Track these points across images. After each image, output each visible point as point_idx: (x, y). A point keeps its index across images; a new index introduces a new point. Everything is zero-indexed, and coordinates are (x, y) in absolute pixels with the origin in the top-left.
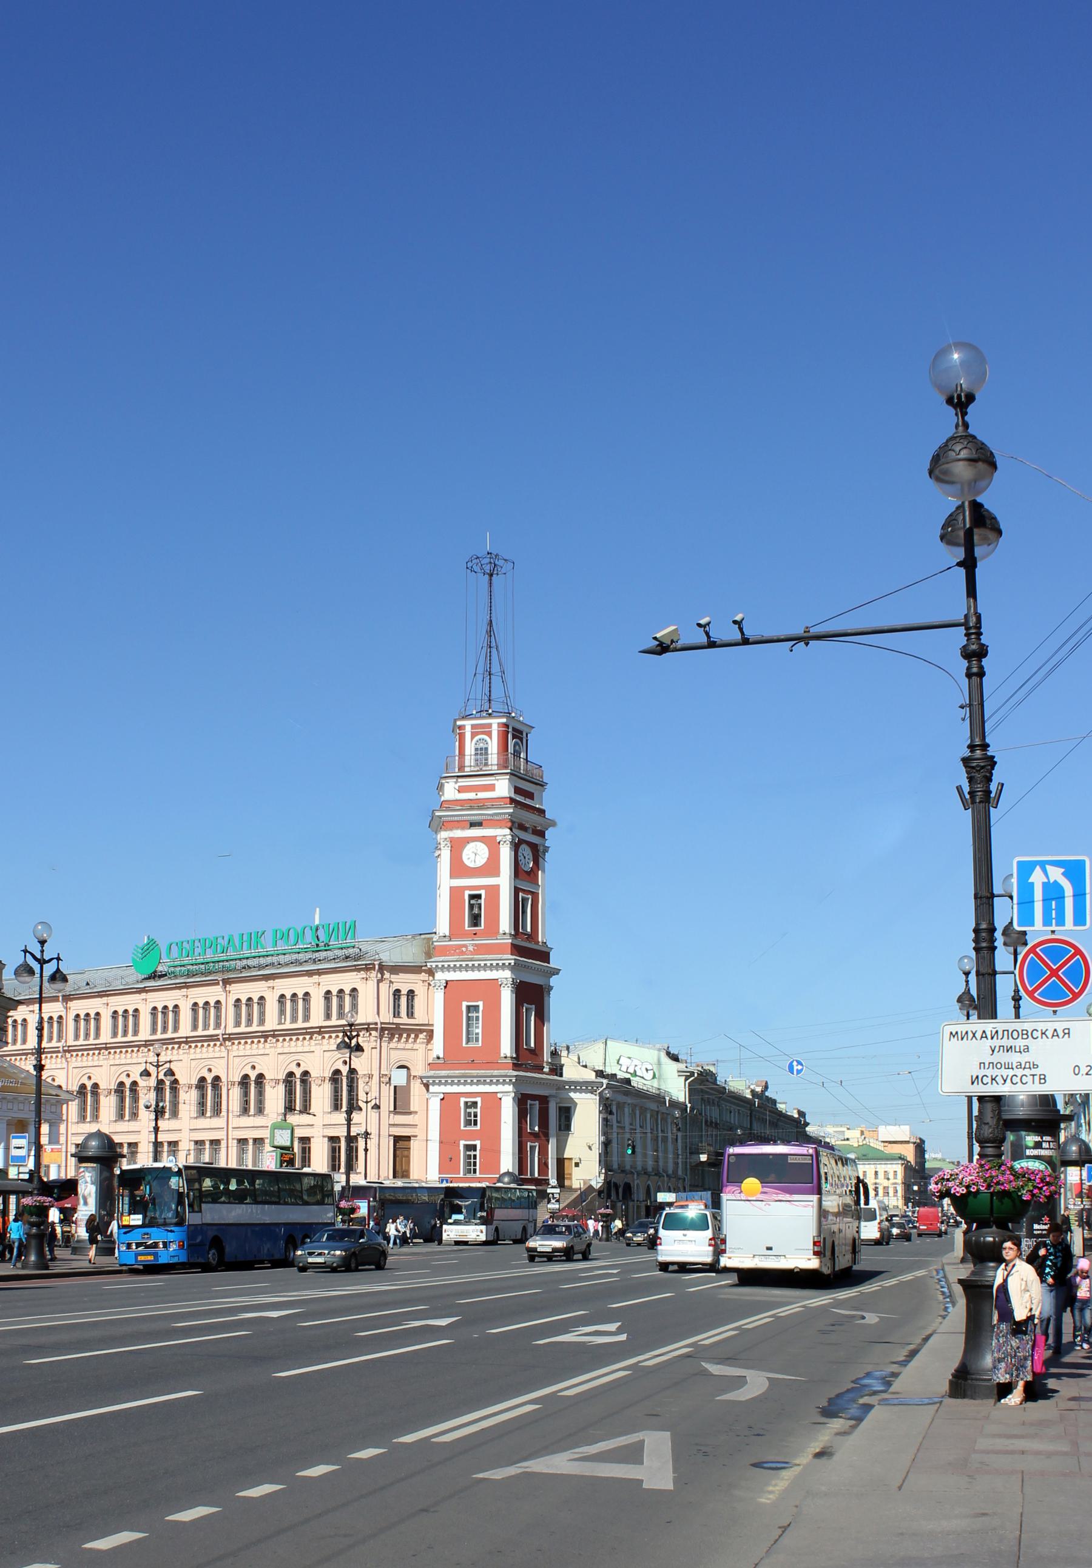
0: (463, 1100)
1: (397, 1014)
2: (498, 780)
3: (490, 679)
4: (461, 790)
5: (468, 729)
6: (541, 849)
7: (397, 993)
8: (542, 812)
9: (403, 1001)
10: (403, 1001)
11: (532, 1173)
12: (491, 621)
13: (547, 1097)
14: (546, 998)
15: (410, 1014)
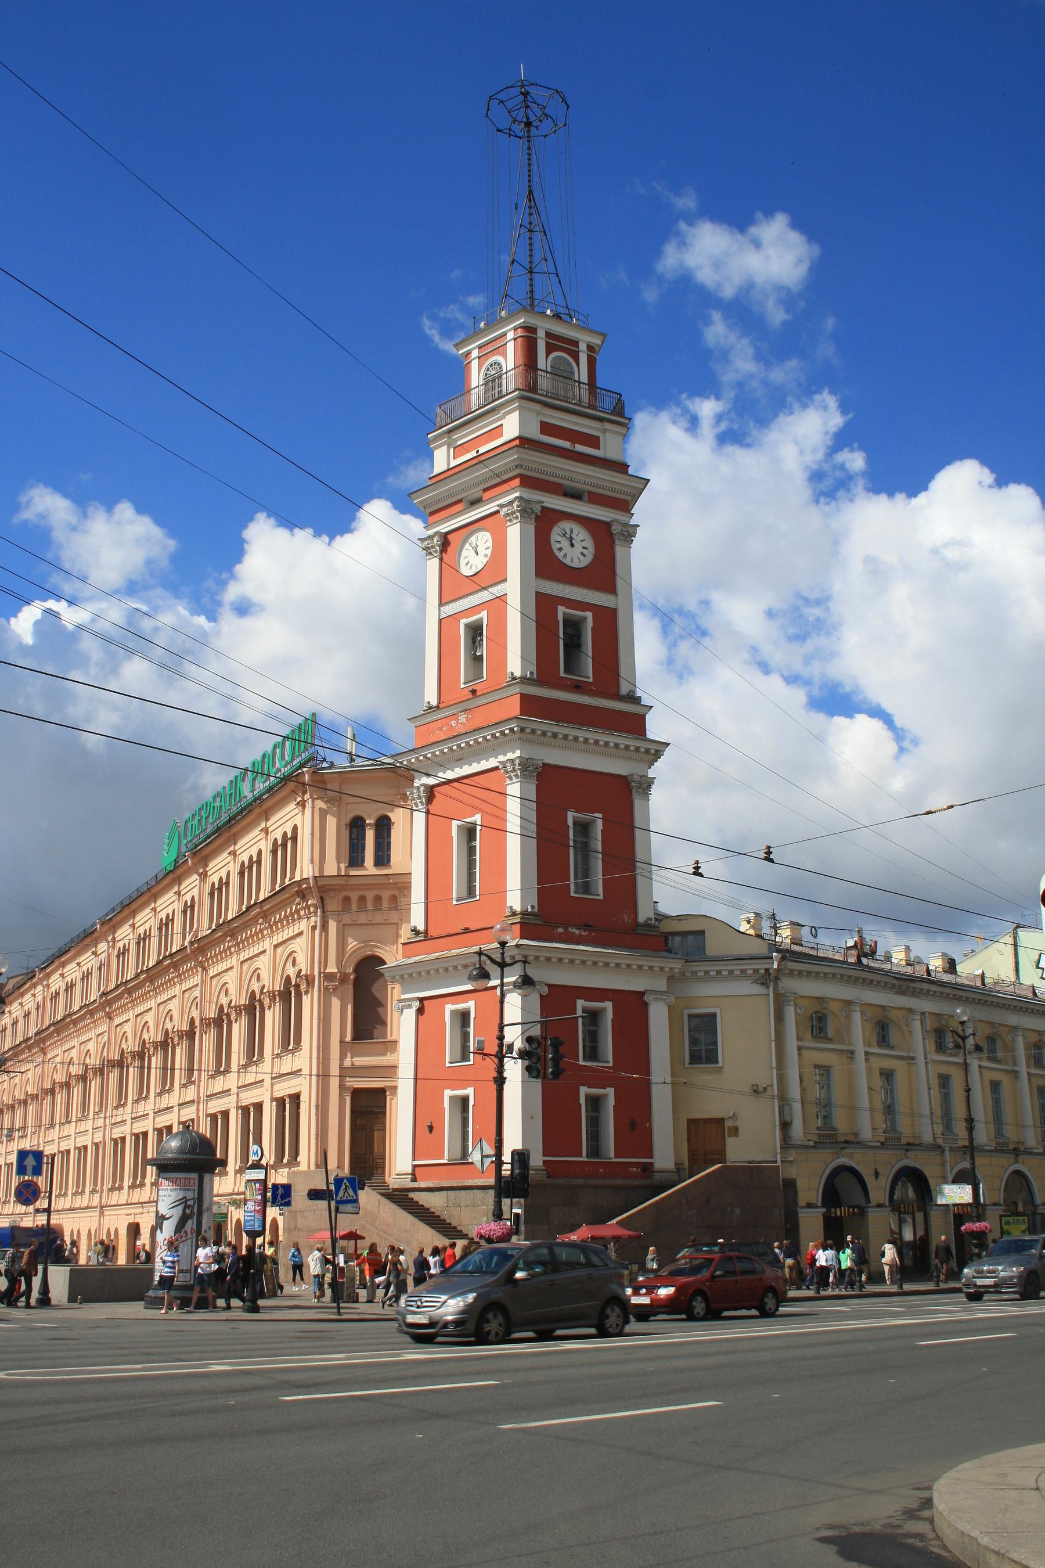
0: (449, 1008)
1: (355, 859)
2: (503, 417)
3: (531, 279)
4: (458, 450)
5: (475, 353)
6: (616, 529)
7: (356, 826)
8: (622, 467)
9: (370, 835)
10: (370, 835)
11: (595, 1150)
12: (530, 192)
13: (642, 994)
14: (637, 803)
15: (382, 858)
